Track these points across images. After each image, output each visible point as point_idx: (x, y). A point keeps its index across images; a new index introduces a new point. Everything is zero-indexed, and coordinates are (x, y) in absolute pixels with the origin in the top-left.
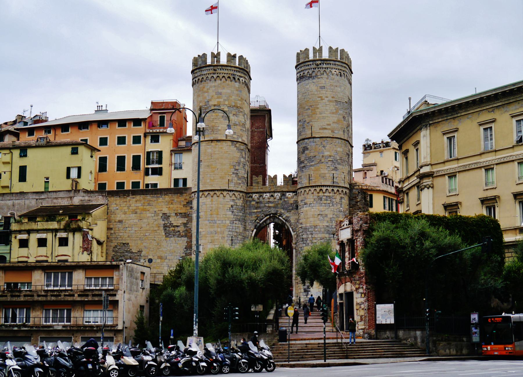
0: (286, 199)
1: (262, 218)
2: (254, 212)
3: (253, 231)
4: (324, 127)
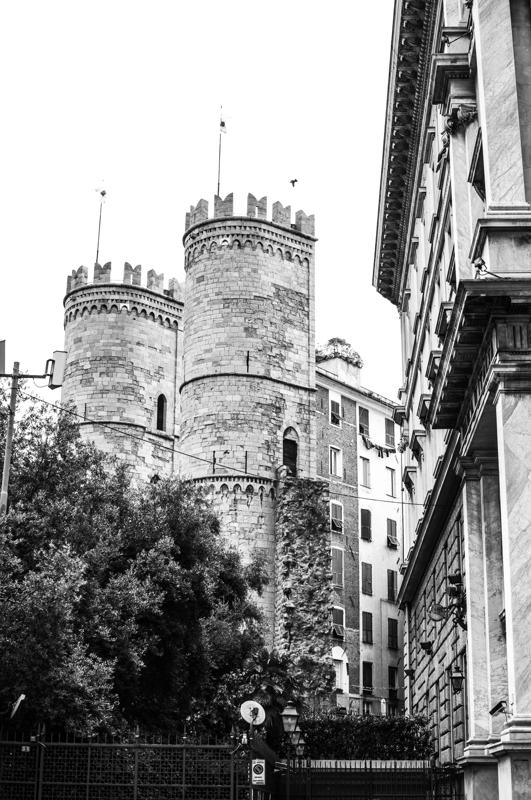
4: (199, 357)
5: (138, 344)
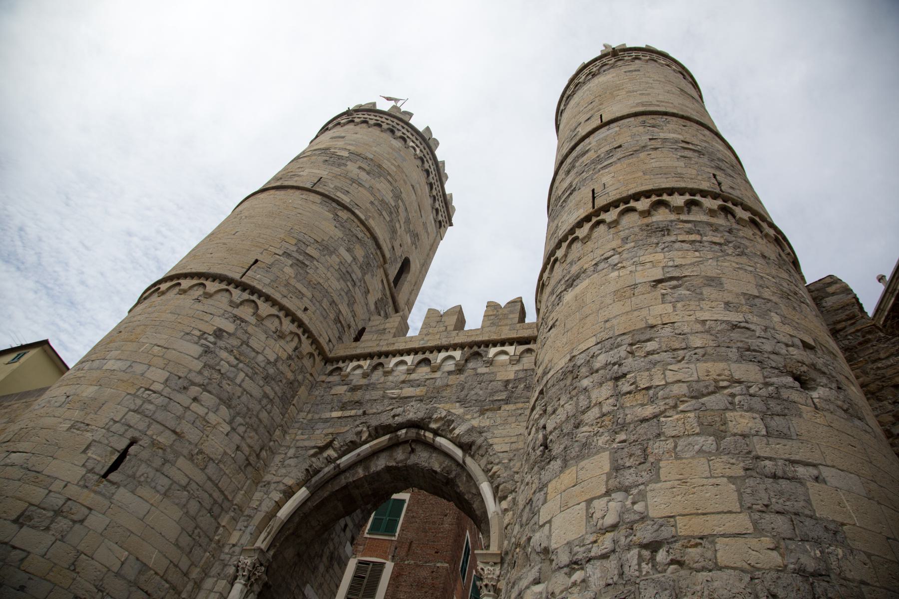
0: (482, 370)
1: (351, 437)
2: (326, 421)
3: (289, 493)
5: (413, 187)
